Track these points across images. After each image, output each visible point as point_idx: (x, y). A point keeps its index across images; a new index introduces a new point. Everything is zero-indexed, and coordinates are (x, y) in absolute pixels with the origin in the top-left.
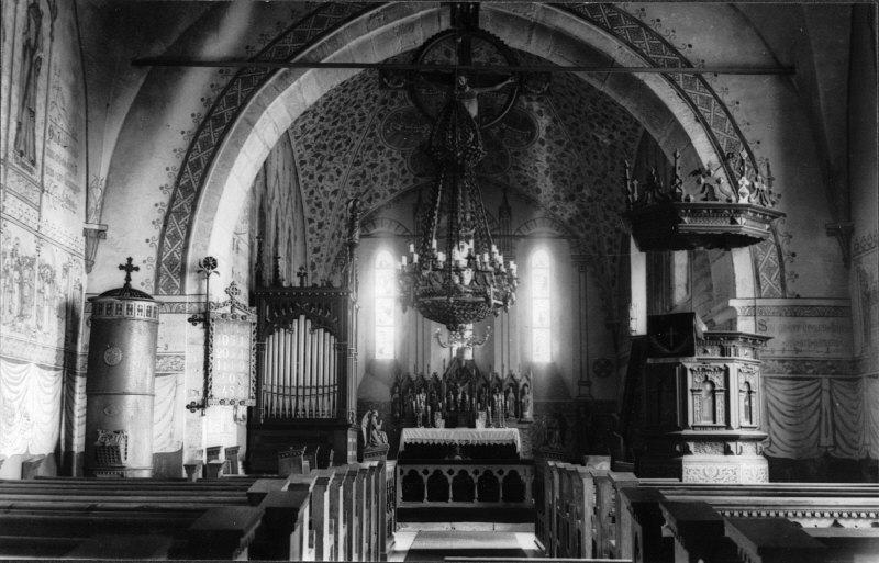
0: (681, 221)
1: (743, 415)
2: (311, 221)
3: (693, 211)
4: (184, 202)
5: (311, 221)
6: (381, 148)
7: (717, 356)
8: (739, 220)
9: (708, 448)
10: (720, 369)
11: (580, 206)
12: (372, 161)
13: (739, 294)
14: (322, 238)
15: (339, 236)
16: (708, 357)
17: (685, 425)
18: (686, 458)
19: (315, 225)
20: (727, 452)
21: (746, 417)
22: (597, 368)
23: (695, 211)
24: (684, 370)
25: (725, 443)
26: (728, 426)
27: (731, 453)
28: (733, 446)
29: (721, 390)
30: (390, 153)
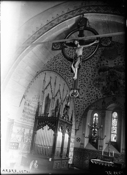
2: (76, 105)
5: (76, 105)
6: (93, 88)
12: (91, 91)
14: (79, 109)
15: (84, 108)
19: (77, 106)
30: (95, 89)
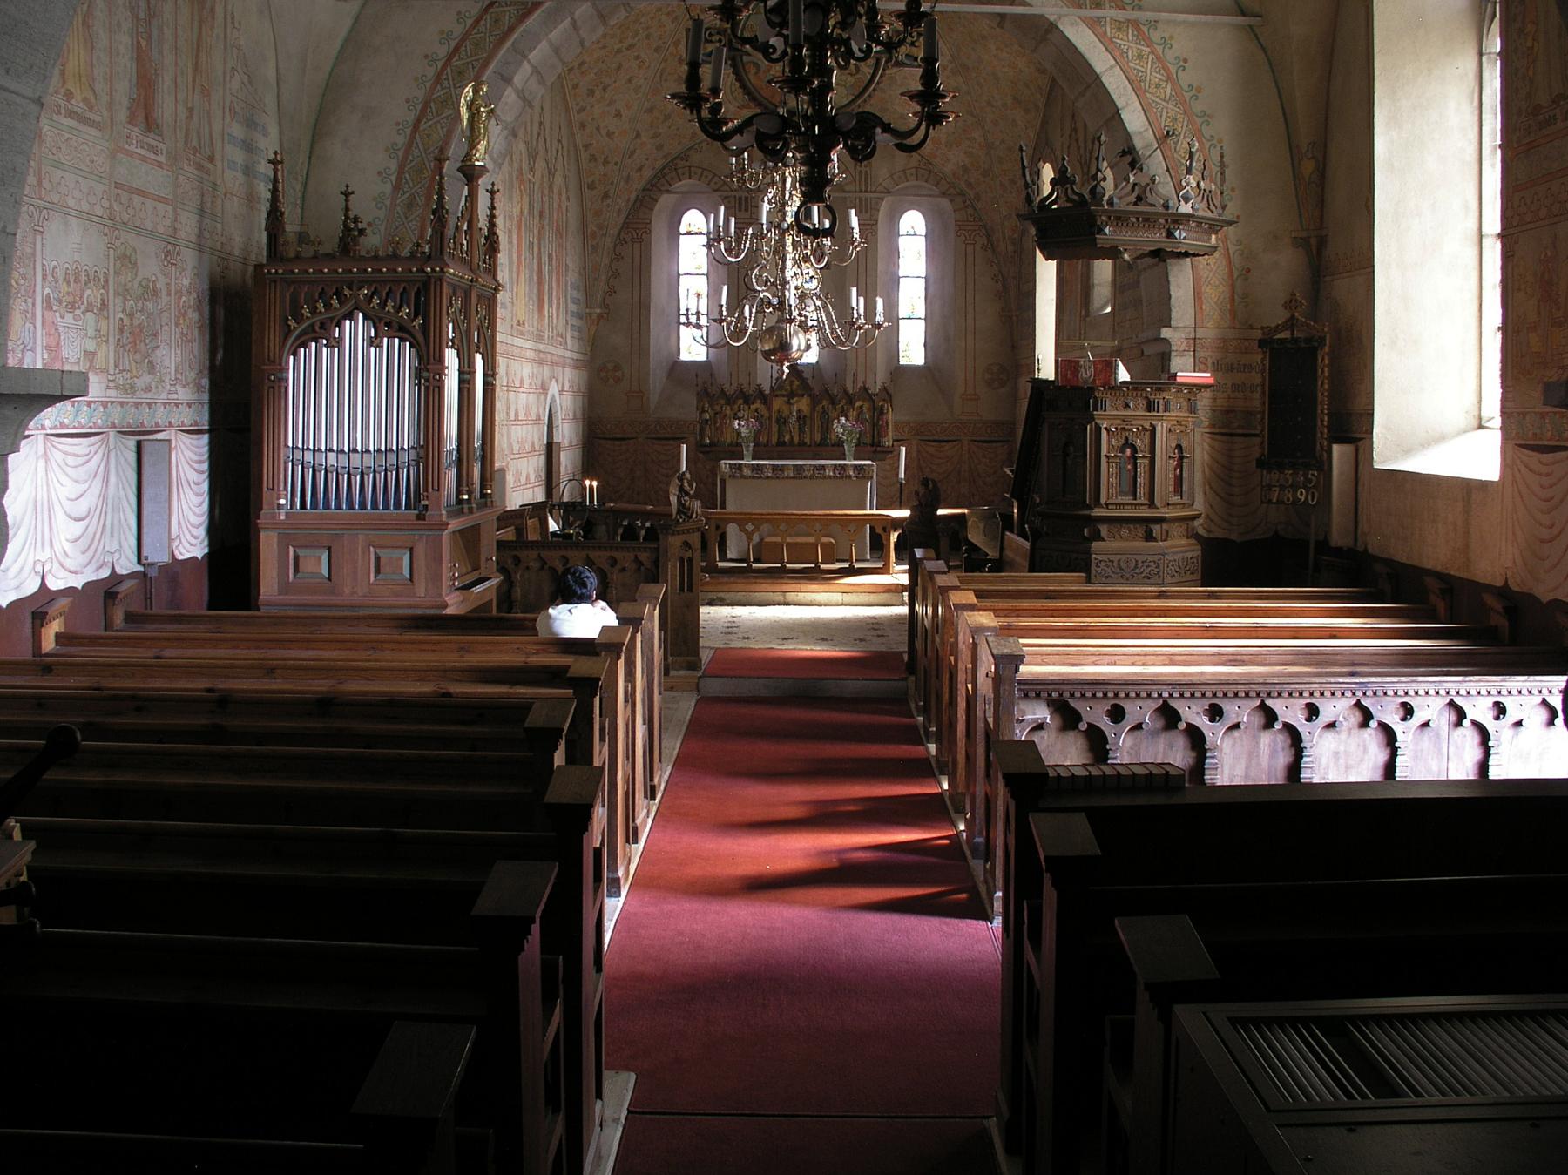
0: (1100, 231)
1: (1171, 489)
3: (1118, 219)
4: (467, 377)
8: (1177, 234)
13: (1173, 323)
17: (1097, 503)
20: (1149, 537)
22: (987, 376)
23: (1120, 219)
24: (1098, 429)
25: (1147, 527)
26: (1152, 505)
27: (1154, 539)
28: (1156, 529)
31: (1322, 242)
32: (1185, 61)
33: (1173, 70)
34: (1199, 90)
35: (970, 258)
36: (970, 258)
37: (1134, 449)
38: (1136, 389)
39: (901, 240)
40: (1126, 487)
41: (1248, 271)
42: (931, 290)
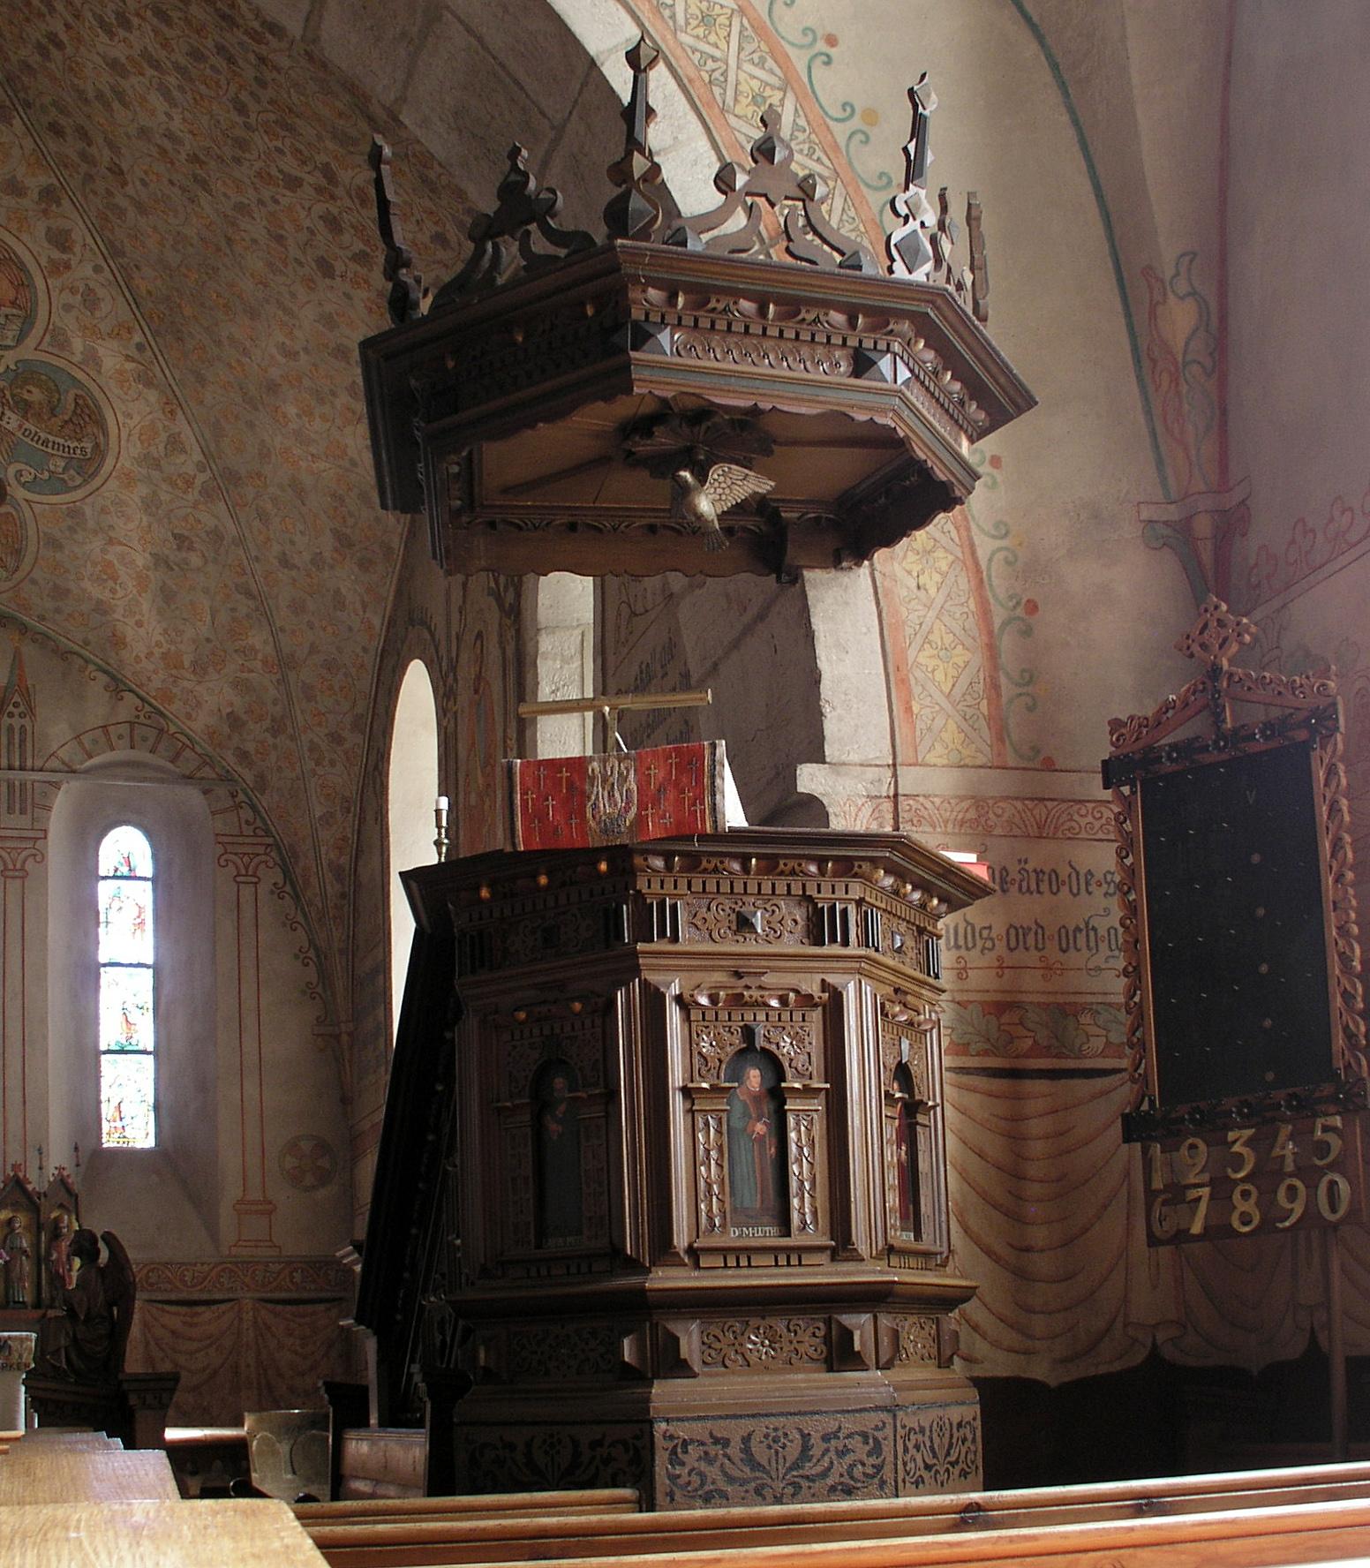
0: (643, 337)
7: (791, 943)
9: (754, 1342)
10: (807, 1000)
11: (239, 685)
16: (751, 947)
17: (662, 1247)
18: (664, 1393)
20: (840, 1355)
21: (904, 1217)
22: (290, 1162)
24: (654, 1001)
25: (828, 1319)
26: (841, 1246)
28: (860, 1325)
29: (808, 1092)
31: (1231, 524)
32: (832, 41)
33: (799, 60)
34: (871, 116)
35: (248, 913)
36: (248, 913)
37: (774, 1066)
38: (770, 865)
39: (105, 890)
40: (753, 1196)
41: (1032, 607)
42: (166, 990)
